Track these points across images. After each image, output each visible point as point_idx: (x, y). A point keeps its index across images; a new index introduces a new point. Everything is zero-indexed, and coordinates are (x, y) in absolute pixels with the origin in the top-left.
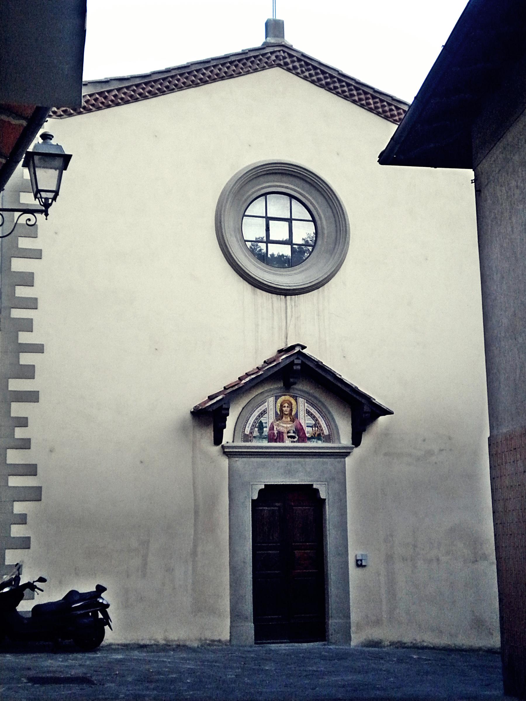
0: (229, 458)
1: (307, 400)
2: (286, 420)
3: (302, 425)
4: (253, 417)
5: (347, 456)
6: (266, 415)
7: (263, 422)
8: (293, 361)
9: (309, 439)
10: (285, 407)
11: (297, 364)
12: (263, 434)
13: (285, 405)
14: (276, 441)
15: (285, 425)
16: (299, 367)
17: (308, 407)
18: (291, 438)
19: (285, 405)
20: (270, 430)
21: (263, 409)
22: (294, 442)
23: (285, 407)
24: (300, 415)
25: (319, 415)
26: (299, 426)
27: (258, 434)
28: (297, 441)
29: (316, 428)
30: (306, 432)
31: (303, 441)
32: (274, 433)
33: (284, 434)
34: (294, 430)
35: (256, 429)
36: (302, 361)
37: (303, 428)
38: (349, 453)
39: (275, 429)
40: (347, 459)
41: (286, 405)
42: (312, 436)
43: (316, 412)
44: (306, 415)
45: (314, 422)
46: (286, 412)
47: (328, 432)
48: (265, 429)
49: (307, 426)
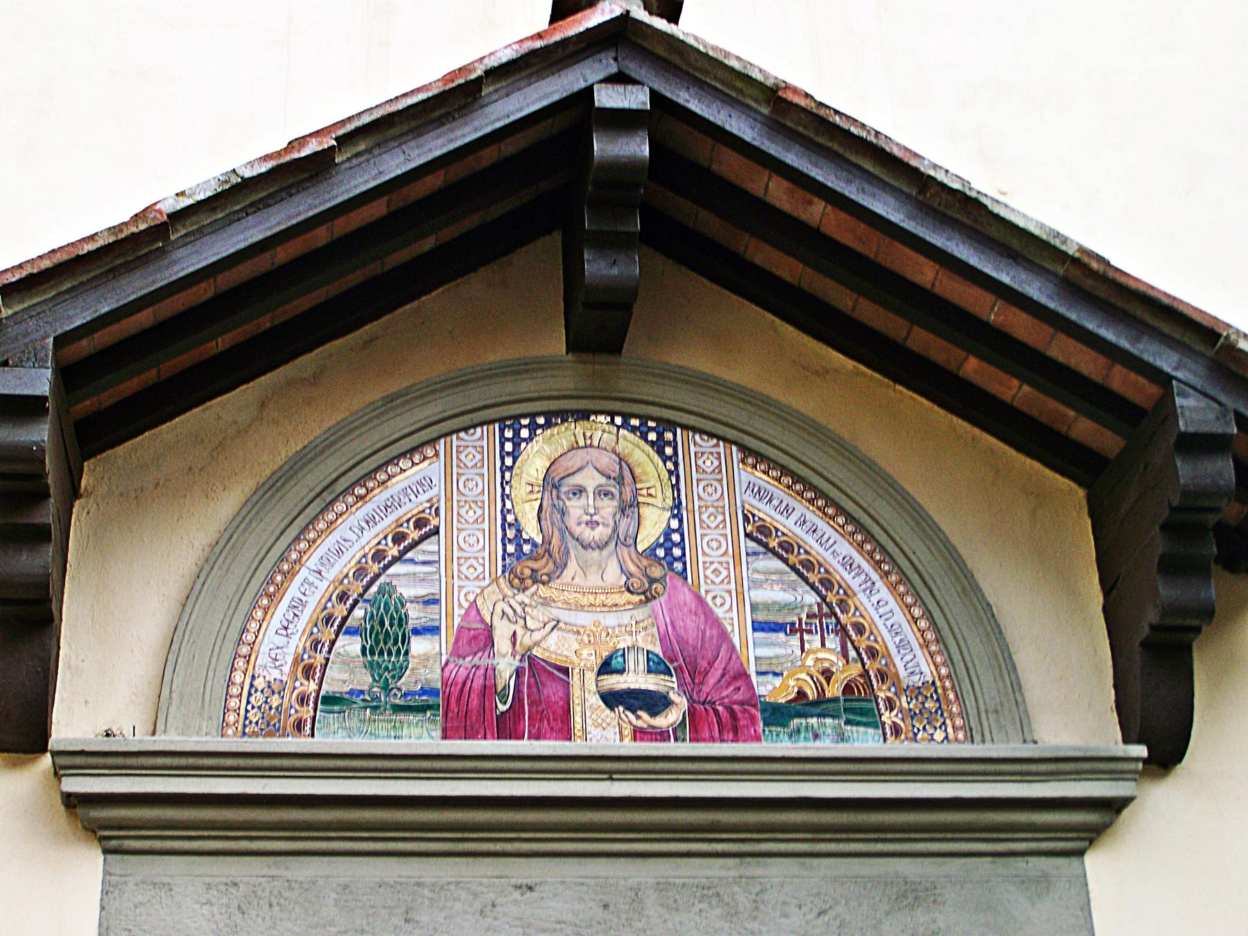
0: (106, 851)
1: (742, 448)
2: (593, 580)
3: (719, 612)
4: (326, 561)
5: (1092, 835)
7: (407, 591)
8: (588, 92)
9: (778, 715)
10: (579, 491)
11: (622, 121)
12: (406, 682)
13: (577, 480)
14: (507, 727)
15: (583, 619)
16: (638, 147)
17: (759, 493)
18: (630, 708)
19: (577, 480)
20: (456, 653)
21: (410, 508)
22: (662, 736)
23: (579, 491)
24: (703, 544)
25: (845, 548)
26: (690, 627)
27: (364, 680)
29: (833, 642)
30: (752, 671)
31: (733, 728)
32: (490, 672)
33: (575, 681)
34: (658, 650)
35: (351, 646)
36: (655, 96)
37: (724, 636)
38: (1115, 806)
39: (502, 643)
40: (1096, 863)
41: (590, 480)
42: (801, 694)
44: (746, 545)
45: (811, 598)
46: (592, 524)
47: (924, 668)
48: (419, 646)
49: (758, 627)
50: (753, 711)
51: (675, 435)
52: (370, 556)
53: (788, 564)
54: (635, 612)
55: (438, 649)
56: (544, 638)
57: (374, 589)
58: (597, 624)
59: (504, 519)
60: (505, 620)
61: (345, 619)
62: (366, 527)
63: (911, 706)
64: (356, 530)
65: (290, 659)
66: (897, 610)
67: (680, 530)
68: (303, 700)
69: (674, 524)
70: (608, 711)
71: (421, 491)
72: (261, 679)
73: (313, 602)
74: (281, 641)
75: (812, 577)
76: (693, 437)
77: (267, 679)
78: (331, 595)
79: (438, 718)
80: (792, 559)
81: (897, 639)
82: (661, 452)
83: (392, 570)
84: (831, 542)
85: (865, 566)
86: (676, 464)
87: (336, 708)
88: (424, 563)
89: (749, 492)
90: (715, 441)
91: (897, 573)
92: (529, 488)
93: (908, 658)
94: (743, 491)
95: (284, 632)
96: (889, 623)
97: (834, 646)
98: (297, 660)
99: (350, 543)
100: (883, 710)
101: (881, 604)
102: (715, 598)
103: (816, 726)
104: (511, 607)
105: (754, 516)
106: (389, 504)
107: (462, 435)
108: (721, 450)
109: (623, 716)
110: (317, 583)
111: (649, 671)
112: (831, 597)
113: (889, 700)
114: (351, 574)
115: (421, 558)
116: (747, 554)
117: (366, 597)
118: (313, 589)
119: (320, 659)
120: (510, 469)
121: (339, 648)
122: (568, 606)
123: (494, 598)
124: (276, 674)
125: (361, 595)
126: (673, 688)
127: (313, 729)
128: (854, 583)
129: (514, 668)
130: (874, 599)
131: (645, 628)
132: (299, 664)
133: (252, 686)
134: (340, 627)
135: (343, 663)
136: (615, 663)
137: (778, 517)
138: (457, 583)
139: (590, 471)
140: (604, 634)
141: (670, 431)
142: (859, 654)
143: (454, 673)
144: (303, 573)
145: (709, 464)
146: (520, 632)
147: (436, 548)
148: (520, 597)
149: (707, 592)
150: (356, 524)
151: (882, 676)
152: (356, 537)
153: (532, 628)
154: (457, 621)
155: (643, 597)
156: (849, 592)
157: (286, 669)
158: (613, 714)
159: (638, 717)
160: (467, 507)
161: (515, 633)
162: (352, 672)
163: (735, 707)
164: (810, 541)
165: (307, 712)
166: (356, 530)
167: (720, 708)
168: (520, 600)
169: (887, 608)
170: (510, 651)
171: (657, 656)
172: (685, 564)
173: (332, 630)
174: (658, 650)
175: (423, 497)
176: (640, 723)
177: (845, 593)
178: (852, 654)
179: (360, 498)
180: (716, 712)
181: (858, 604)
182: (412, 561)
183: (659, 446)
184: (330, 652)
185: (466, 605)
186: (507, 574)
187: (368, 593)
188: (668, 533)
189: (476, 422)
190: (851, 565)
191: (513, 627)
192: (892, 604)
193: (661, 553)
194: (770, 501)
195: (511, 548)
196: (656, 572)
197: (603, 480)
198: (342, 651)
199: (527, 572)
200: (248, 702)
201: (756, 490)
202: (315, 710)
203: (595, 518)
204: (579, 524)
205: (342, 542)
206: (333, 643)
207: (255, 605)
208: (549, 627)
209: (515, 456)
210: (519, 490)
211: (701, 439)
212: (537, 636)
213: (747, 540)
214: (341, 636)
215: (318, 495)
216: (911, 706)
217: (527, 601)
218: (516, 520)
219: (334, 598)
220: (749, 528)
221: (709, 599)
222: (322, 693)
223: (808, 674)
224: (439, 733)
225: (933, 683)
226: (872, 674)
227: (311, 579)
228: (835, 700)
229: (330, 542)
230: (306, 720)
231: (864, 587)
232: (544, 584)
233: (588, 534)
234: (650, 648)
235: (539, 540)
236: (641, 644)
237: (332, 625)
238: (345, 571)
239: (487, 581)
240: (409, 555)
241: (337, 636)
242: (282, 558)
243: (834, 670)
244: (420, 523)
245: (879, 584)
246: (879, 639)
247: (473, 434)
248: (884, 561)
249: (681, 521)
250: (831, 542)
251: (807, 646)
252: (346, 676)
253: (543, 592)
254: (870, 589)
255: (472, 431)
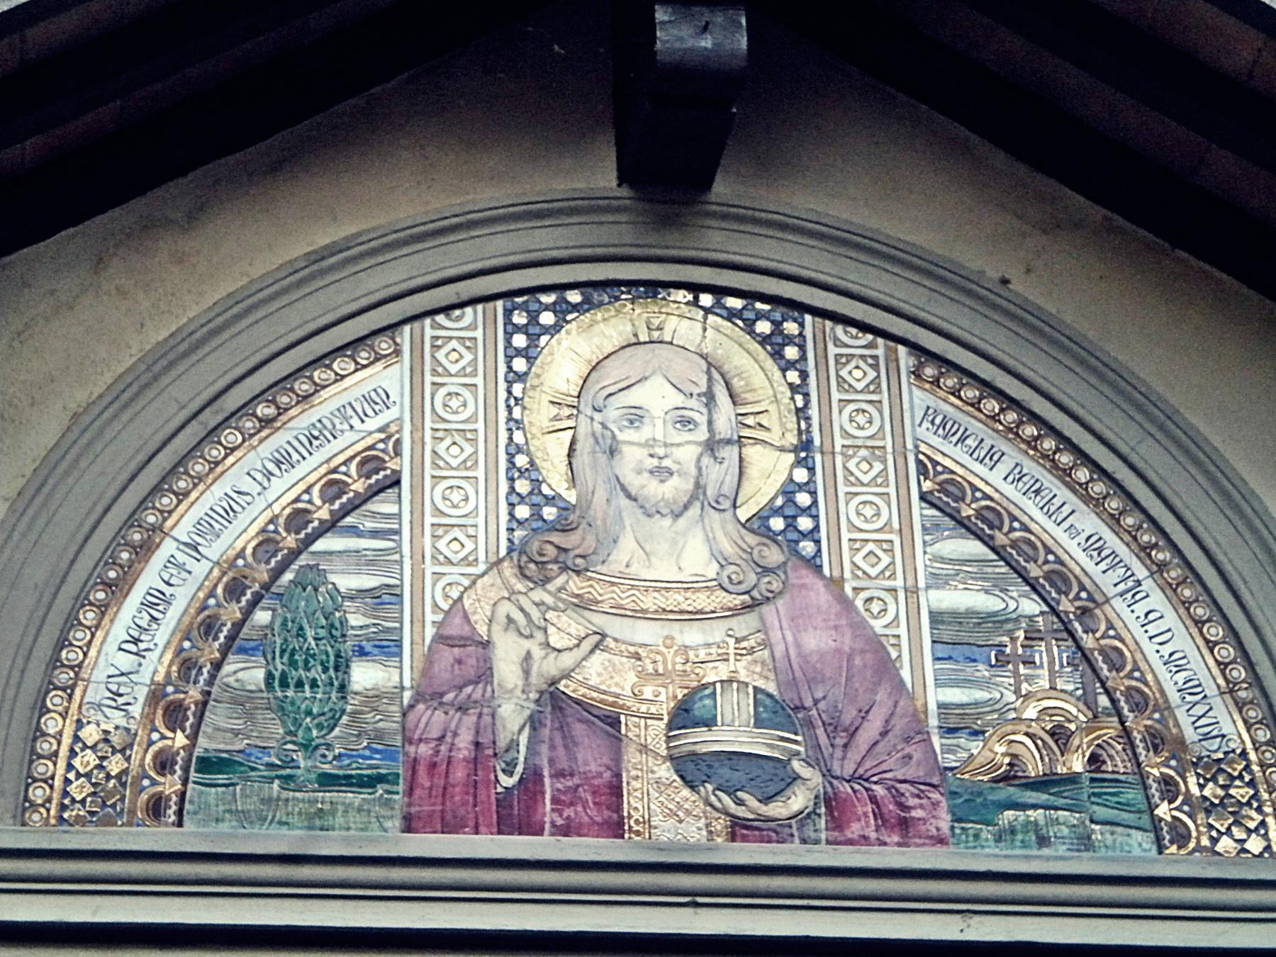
4: (206, 528)
6: (383, 505)
15: (646, 633)
17: (944, 427)
24: (848, 510)
25: (1089, 523)
28: (805, 818)
39: (507, 669)
43: (1050, 482)
46: (662, 473)
48: (364, 676)
50: (935, 796)
51: (802, 325)
52: (281, 520)
53: (993, 549)
54: (733, 622)
55: (397, 678)
56: (578, 665)
57: (288, 576)
58: (669, 641)
59: (511, 461)
60: (512, 636)
61: (238, 626)
62: (276, 471)
63: (1207, 792)
64: (259, 476)
65: (142, 693)
66: (1179, 629)
67: (809, 487)
68: (164, 764)
69: (801, 475)
70: (686, 792)
71: (370, 412)
72: (92, 727)
73: (182, 598)
74: (125, 662)
75: (1034, 571)
76: (832, 329)
77: (103, 726)
78: (216, 586)
79: (396, 797)
80: (1000, 539)
81: (1180, 677)
82: (777, 355)
83: (320, 545)
84: (1066, 510)
85: (1123, 551)
86: (804, 375)
87: (221, 778)
88: (375, 534)
89: (926, 424)
90: (870, 337)
91: (1178, 565)
92: (554, 410)
93: (1199, 710)
94: (918, 421)
95: (133, 648)
96: (1166, 650)
97: (1070, 687)
98: (156, 695)
99: (248, 498)
100: (1156, 800)
101: (1151, 617)
102: (869, 600)
103: (1042, 822)
104: (522, 610)
105: (935, 463)
106: (316, 433)
107: (440, 318)
108: (880, 352)
109: (713, 798)
110: (190, 564)
111: (758, 724)
112: (1065, 605)
113: (1166, 781)
114: (249, 551)
115: (369, 525)
116: (924, 528)
117: (274, 589)
118: (184, 575)
119: (194, 694)
120: (521, 377)
121: (228, 676)
122: (620, 612)
123: (494, 595)
124: (118, 718)
125: (266, 587)
126: (798, 753)
127: (180, 813)
128: (1108, 582)
129: (528, 712)
130: (1141, 608)
131: (751, 651)
132: (157, 704)
133: (77, 738)
134: (231, 638)
135: (235, 701)
136: (699, 708)
137: (977, 468)
138: (430, 568)
139: (658, 382)
140: (679, 659)
141: (795, 320)
142: (1113, 701)
143: (424, 720)
144: (168, 548)
145: (858, 376)
146: (537, 653)
147: (393, 509)
148: (538, 595)
149: (856, 590)
150: (260, 468)
151: (1156, 741)
152: (259, 489)
153: (558, 646)
154: (430, 632)
155: (746, 597)
156: (1099, 598)
157: (136, 710)
158: (695, 797)
159: (740, 803)
160: (448, 441)
161: (528, 656)
162: (250, 716)
163: (903, 787)
164: (1031, 507)
165: (170, 785)
166: (259, 476)
167: (879, 790)
168: (537, 599)
169: (1161, 626)
170: (520, 683)
171: (770, 696)
172: (818, 542)
173: (216, 644)
174: (771, 688)
175: (373, 423)
176: (740, 812)
177: (1091, 598)
178: (1104, 701)
179: (266, 422)
180: (873, 799)
181: (1112, 616)
182: (354, 531)
183: (774, 344)
184: (210, 682)
185: (446, 607)
186: (515, 555)
187: (278, 583)
188: (790, 488)
189: (465, 297)
190: (1100, 550)
191: (527, 644)
192: (1171, 619)
193: (777, 524)
194: (962, 440)
195: (523, 512)
196: (774, 556)
197: (679, 400)
198: (231, 680)
199: (551, 551)
200: (70, 767)
201: (938, 421)
202: (185, 782)
203: (666, 463)
204: (639, 472)
205: (235, 496)
206: (217, 666)
207: (81, 601)
208: (587, 645)
209: (528, 354)
210: (540, 414)
211: (846, 332)
212: (567, 660)
213: (924, 505)
214: (231, 657)
215: (195, 415)
216: (1207, 792)
217: (549, 600)
218: (532, 463)
219: (220, 590)
220: (927, 485)
221: (859, 603)
222: (198, 752)
223: (1027, 734)
224: (397, 823)
225: (1244, 754)
226: (1137, 736)
227: (181, 557)
228: (1073, 779)
229: (212, 497)
230: (168, 798)
231: (1122, 587)
232: (578, 573)
233: (656, 490)
234: (760, 683)
235: (571, 497)
236: (743, 676)
237: (216, 638)
238: (239, 544)
239: (482, 567)
240: (349, 520)
241: (224, 655)
242: (132, 521)
243: (1073, 727)
244: (370, 463)
245: (1148, 585)
246: (1149, 677)
247: (459, 319)
248: (1155, 546)
249: (811, 470)
250: (1066, 510)
251: (1025, 687)
252: (238, 724)
253: (575, 584)
254: (1134, 591)
255: (457, 312)
